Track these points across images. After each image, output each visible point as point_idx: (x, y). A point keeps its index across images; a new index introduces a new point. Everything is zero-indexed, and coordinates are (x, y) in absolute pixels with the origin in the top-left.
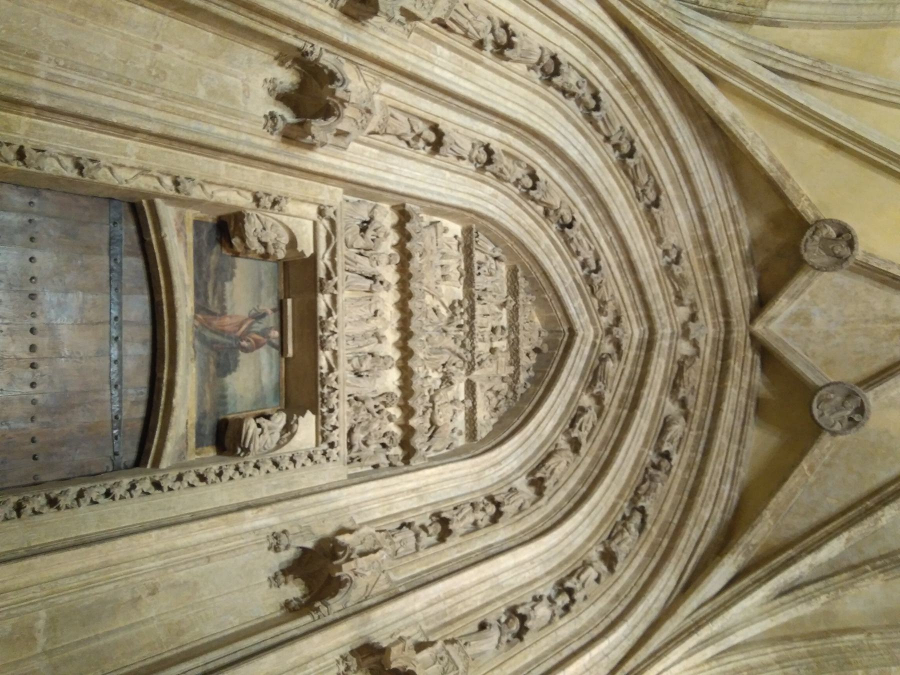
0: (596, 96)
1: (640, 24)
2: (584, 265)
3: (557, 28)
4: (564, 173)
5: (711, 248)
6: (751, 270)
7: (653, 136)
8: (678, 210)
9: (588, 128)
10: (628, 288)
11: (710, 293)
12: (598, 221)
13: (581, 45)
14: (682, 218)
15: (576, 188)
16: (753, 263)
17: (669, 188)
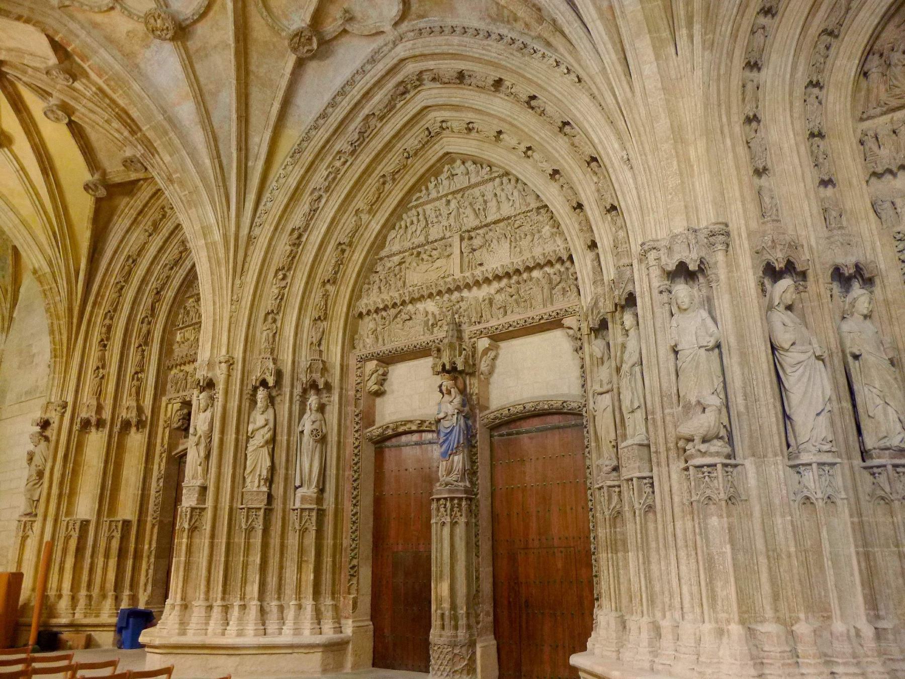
0: (106, 314)
1: (75, 321)
2: (172, 268)
3: (90, 349)
4: (139, 305)
5: (136, 219)
6: (135, 190)
7: (111, 275)
8: (131, 242)
9: (119, 308)
10: (171, 243)
11: (153, 204)
12: (152, 275)
13: (92, 335)
14: (133, 239)
15: (143, 295)
16: (132, 190)
17: (125, 253)
